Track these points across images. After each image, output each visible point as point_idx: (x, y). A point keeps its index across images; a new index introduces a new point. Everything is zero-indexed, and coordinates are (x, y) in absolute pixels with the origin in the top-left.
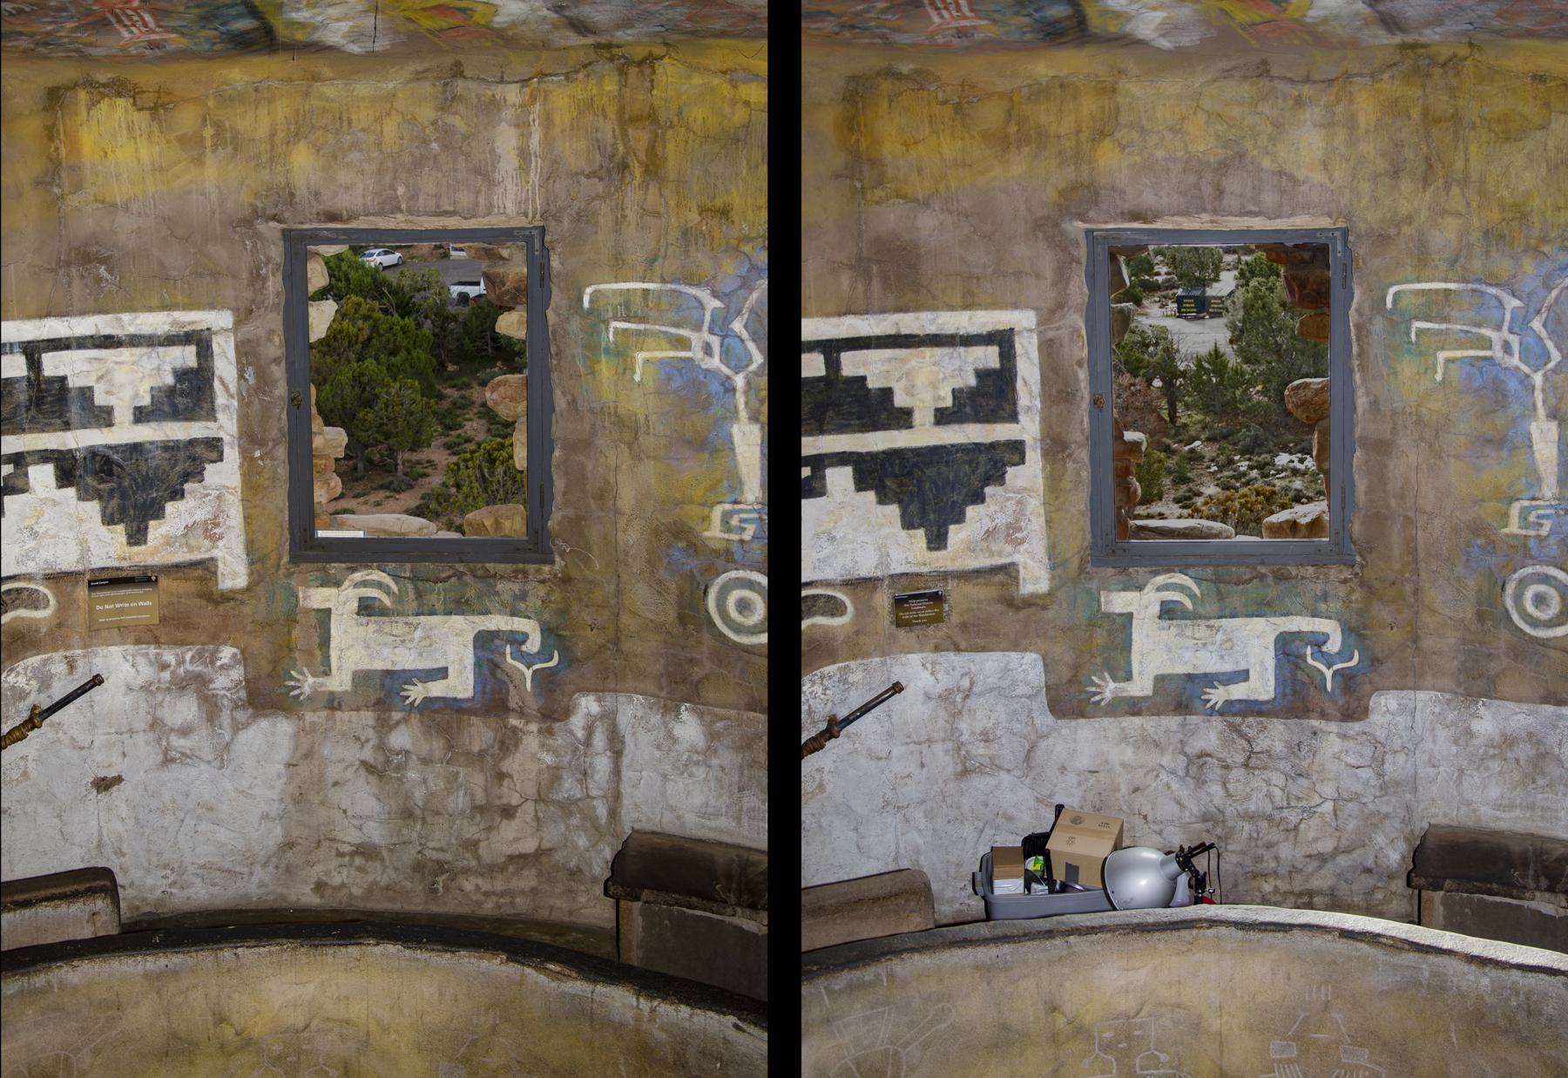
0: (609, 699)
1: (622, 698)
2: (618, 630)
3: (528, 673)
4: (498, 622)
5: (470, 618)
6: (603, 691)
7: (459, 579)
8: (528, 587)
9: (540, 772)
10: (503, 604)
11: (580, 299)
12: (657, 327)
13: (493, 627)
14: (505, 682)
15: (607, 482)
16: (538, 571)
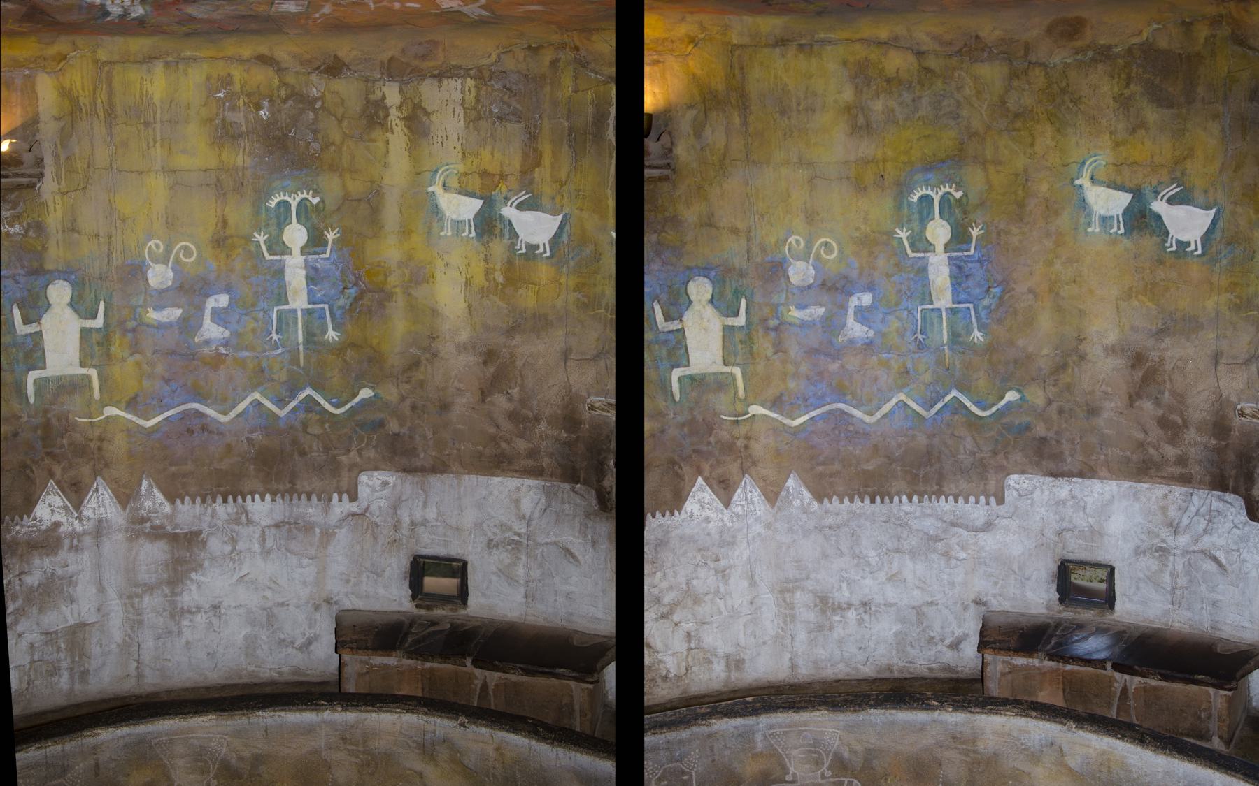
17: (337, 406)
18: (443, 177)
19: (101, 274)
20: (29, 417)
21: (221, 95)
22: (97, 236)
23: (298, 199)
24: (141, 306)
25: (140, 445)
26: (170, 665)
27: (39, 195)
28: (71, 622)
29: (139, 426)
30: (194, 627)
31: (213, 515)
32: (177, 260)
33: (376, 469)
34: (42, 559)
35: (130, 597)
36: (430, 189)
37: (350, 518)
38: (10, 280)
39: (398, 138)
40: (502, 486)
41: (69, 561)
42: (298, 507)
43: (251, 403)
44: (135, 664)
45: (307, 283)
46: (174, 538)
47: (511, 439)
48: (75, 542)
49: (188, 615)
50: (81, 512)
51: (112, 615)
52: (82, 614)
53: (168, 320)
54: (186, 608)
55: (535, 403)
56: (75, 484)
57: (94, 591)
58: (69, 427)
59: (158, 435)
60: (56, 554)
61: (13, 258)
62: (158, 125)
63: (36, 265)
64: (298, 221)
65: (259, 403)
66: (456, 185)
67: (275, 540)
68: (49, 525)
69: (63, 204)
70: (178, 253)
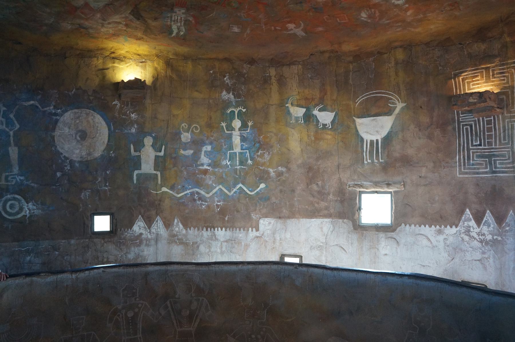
17: (251, 191)
18: (291, 101)
21: (211, 72)
23: (238, 110)
24: (178, 148)
31: (202, 235)
32: (192, 131)
33: (266, 217)
34: (135, 248)
36: (287, 105)
37: (256, 238)
39: (275, 87)
40: (315, 222)
42: (235, 233)
43: (218, 189)
45: (241, 143)
47: (319, 202)
50: (151, 230)
55: (328, 187)
56: (149, 218)
64: (238, 119)
65: (221, 189)
66: (296, 103)
67: (226, 248)
68: (138, 234)
70: (193, 128)
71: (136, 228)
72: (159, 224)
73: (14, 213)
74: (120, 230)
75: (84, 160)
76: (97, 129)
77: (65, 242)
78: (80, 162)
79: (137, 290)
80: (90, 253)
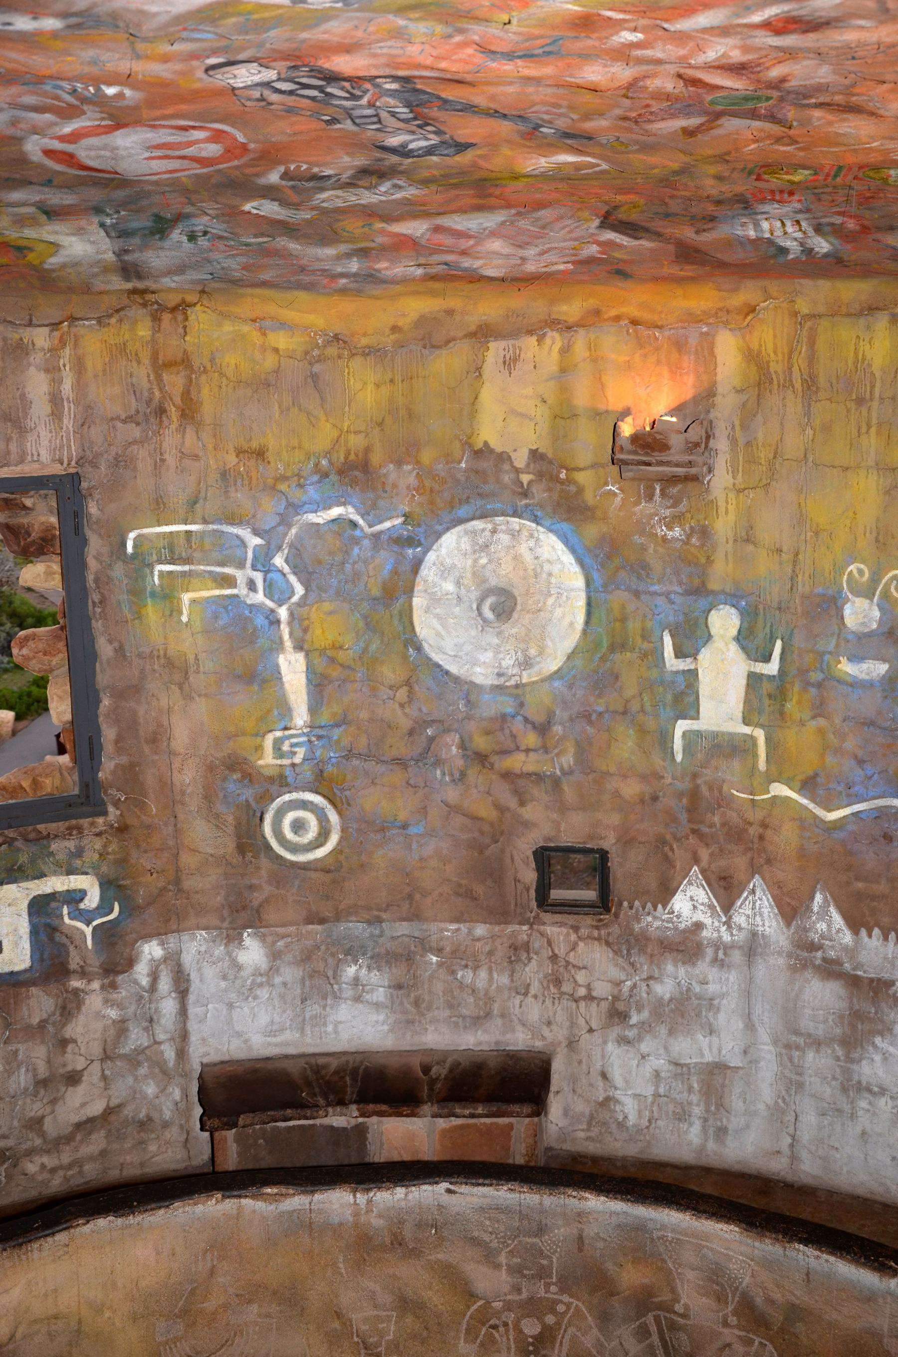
0: (172, 940)
1: (185, 937)
2: (178, 870)
3: (88, 931)
4: (56, 884)
5: (24, 885)
6: (166, 934)
7: (10, 845)
8: (85, 841)
9: (105, 1029)
10: (58, 865)
11: (124, 545)
12: (202, 567)
13: (48, 890)
14: (64, 945)
15: (160, 725)
16: (92, 824)
19: (780, 602)
20: (673, 779)
22: (780, 551)
24: (830, 653)
25: (815, 843)
26: (838, 1156)
27: (707, 490)
28: (708, 1058)
29: (816, 817)
30: (874, 1114)
32: (886, 595)
34: (676, 966)
35: (788, 1047)
38: (663, 598)
41: (710, 978)
44: (790, 1140)
46: (854, 982)
48: (721, 955)
49: (866, 1095)
50: (730, 917)
51: (762, 1064)
52: (724, 1052)
53: (867, 677)
54: (864, 1084)
56: (724, 878)
57: (741, 1025)
58: (723, 801)
59: (841, 835)
60: (694, 964)
61: (668, 570)
62: (875, 404)
63: (696, 582)
69: (738, 504)
70: (888, 585)
71: (681, 903)
72: (759, 902)
73: (304, 845)
74: (631, 907)
75: (507, 684)
76: (550, 583)
77: (458, 930)
78: (499, 689)
79: (549, 1258)
80: (534, 963)
